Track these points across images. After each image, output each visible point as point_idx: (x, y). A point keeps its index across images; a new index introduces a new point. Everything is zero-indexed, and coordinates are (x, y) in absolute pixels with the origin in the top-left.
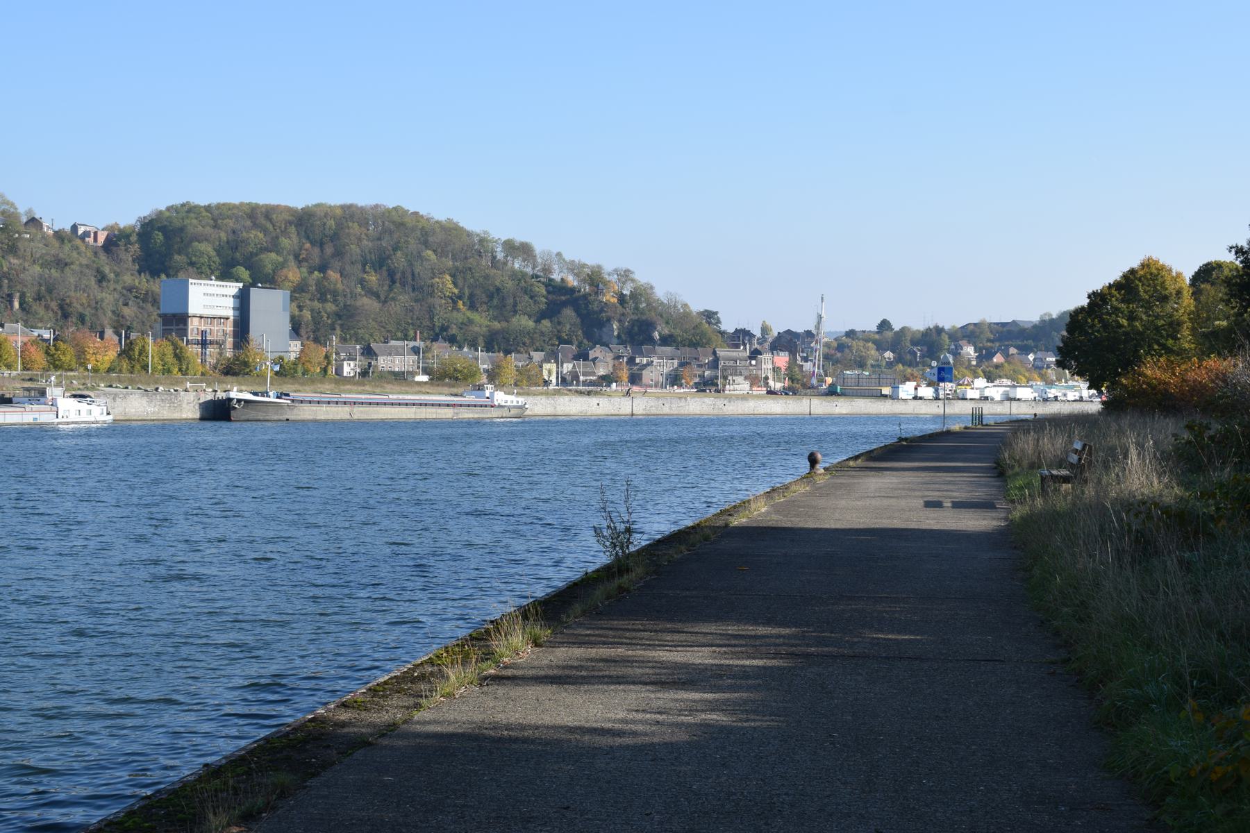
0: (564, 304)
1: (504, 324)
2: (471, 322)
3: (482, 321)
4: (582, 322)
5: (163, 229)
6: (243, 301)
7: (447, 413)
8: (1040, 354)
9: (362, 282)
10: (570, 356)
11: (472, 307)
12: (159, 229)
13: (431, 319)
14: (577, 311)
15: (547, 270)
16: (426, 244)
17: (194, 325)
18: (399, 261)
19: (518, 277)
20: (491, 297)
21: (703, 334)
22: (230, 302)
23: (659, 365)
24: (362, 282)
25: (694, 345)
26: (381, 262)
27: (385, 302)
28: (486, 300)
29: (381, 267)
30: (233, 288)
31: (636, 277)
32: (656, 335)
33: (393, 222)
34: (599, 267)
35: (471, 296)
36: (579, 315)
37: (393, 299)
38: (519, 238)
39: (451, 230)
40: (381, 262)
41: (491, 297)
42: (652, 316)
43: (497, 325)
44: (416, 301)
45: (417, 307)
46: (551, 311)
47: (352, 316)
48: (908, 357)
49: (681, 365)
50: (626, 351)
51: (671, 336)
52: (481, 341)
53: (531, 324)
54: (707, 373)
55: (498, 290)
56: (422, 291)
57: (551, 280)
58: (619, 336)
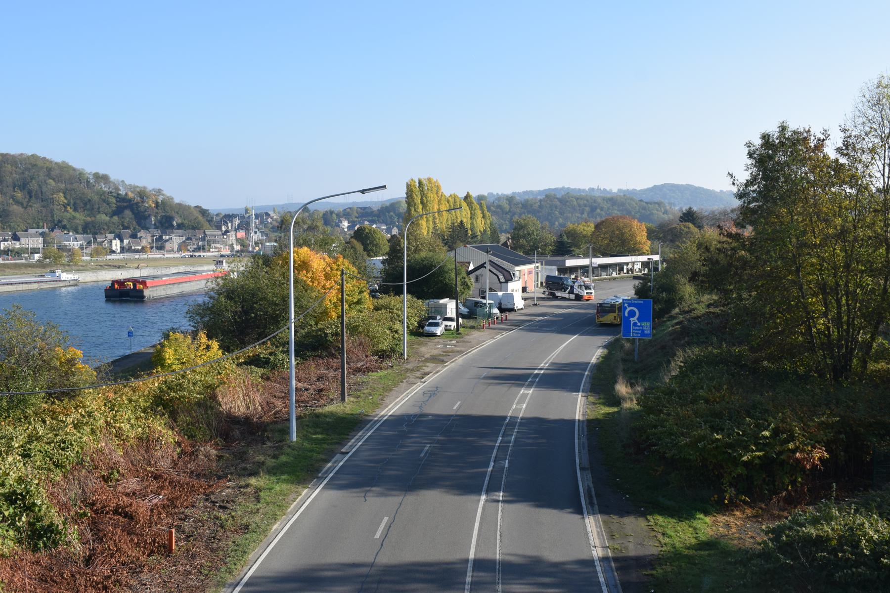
0: (126, 208)
1: (93, 219)
2: (74, 218)
3: (81, 217)
4: (136, 217)
7: (35, 286)
8: (378, 225)
9: (13, 197)
11: (75, 210)
13: (52, 216)
15: (117, 189)
16: (49, 176)
18: (34, 186)
19: (101, 194)
20: (85, 204)
21: (199, 223)
23: (176, 240)
24: (13, 197)
25: (194, 228)
26: (23, 186)
27: (26, 208)
28: (82, 205)
29: (24, 188)
31: (164, 192)
32: (175, 224)
33: (31, 164)
34: (145, 188)
35: (75, 204)
36: (133, 213)
37: (31, 206)
38: (102, 171)
39: (64, 168)
40: (23, 186)
41: (85, 204)
43: (89, 219)
44: (44, 207)
45: (44, 210)
46: (118, 212)
47: (7, 216)
49: (187, 239)
50: (158, 233)
51: (182, 224)
53: (108, 218)
55: (89, 200)
56: (47, 202)
57: (119, 194)
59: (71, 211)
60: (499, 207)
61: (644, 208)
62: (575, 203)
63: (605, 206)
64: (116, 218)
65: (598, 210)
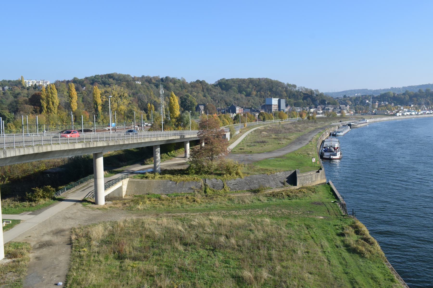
5: (224, 84)
12: (224, 84)
14: (310, 98)
17: (273, 106)
18: (274, 89)
22: (277, 102)
25: (334, 104)
26: (271, 90)
30: (277, 99)
42: (325, 99)
43: (295, 101)
53: (302, 101)
64: (305, 101)
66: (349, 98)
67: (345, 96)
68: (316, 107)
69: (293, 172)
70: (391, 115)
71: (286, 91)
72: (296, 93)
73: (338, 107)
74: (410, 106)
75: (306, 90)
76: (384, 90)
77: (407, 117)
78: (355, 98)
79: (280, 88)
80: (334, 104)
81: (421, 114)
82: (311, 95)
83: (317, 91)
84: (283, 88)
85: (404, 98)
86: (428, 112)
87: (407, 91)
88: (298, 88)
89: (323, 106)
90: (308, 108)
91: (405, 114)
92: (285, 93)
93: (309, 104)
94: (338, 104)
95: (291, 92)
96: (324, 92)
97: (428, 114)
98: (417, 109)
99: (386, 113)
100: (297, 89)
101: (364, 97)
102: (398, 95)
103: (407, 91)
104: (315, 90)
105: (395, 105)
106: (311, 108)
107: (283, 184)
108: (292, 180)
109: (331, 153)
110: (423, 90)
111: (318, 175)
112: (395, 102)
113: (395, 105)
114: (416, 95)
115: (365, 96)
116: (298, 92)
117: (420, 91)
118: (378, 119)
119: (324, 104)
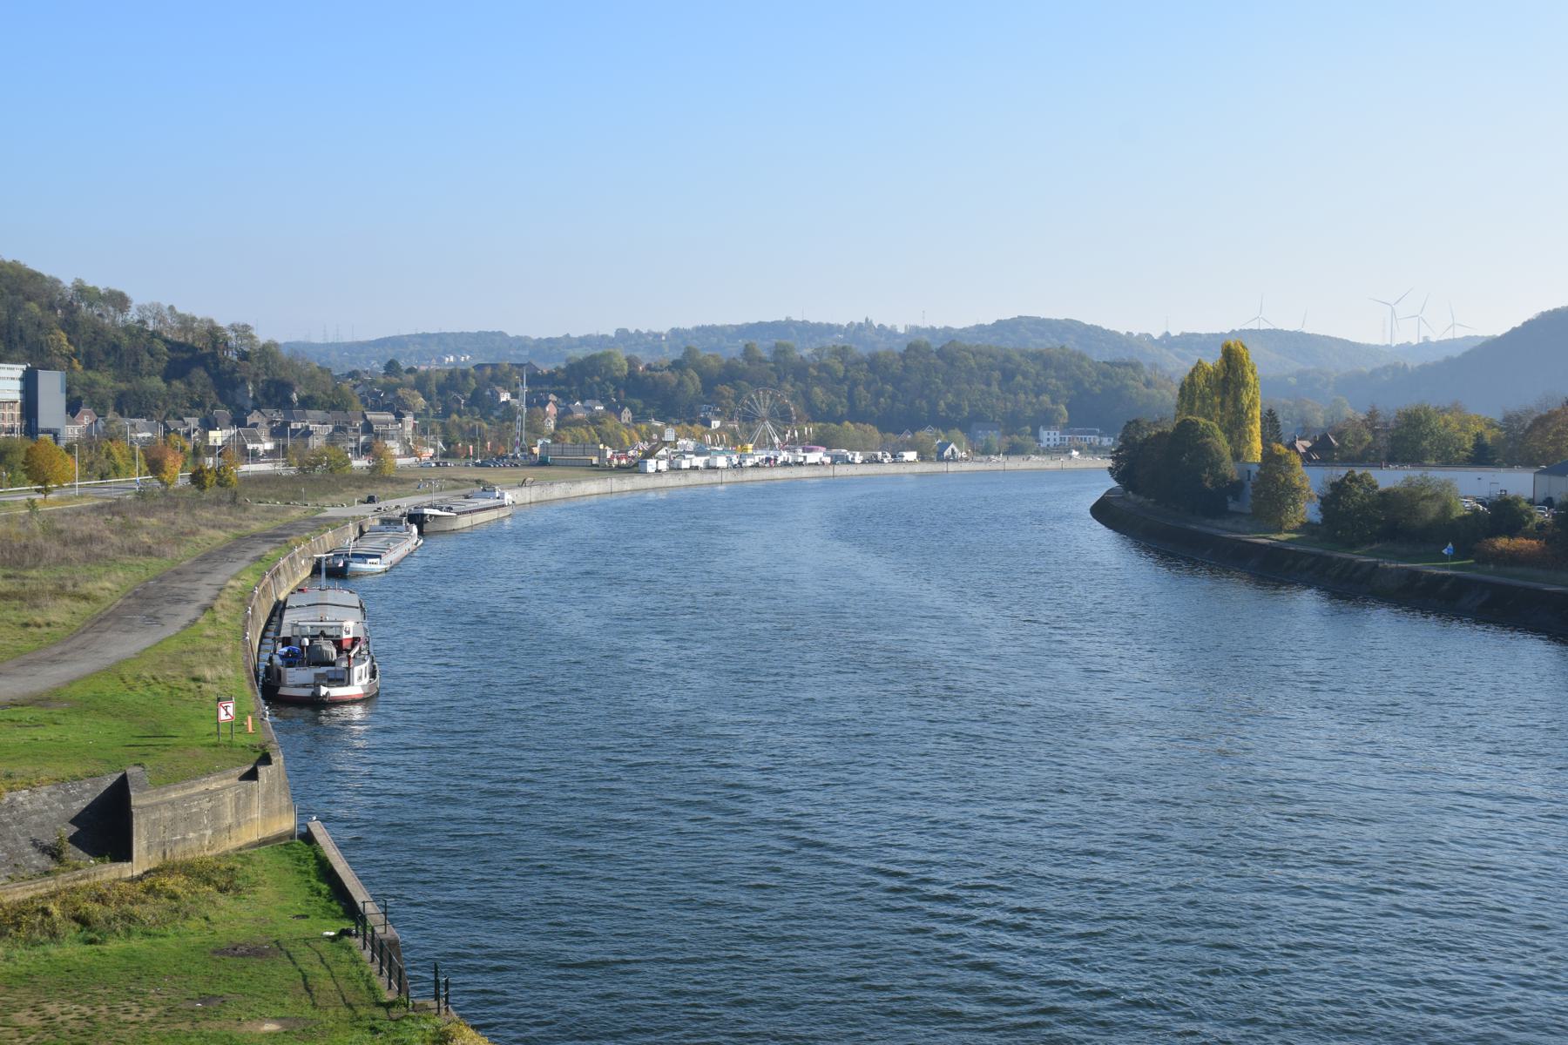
6: (29, 384)
10: (227, 422)
14: (207, 369)
22: (17, 385)
25: (334, 407)
30: (18, 370)
32: (294, 397)
36: (210, 375)
43: (123, 386)
48: (455, 406)
49: (336, 429)
51: (310, 397)
52: (110, 402)
53: (163, 386)
54: (362, 439)
58: (255, 398)
59: (79, 367)
60: (823, 367)
61: (1106, 375)
62: (973, 363)
63: (1032, 369)
64: (178, 385)
65: (1019, 378)
66: (411, 378)
67: (391, 367)
68: (239, 421)
69: (109, 781)
70: (620, 468)
71: (71, 325)
72: (126, 341)
73: (359, 424)
74: (707, 423)
75: (186, 323)
76: (585, 341)
77: (695, 478)
78: (442, 377)
79: (33, 306)
80: (335, 404)
81: (756, 466)
82: (213, 355)
83: (244, 331)
84: (52, 307)
85: (680, 383)
86: (784, 456)
87: (689, 352)
88: (141, 309)
89: (279, 417)
90: (193, 422)
91: (685, 464)
92: (63, 336)
93: (199, 405)
94: (357, 405)
95: (98, 332)
96: (281, 340)
97: (786, 464)
98: (735, 441)
99: (595, 460)
100: (132, 316)
101: (488, 371)
102: (648, 367)
103: (689, 352)
104: (233, 328)
105: (639, 417)
106: (209, 424)
107: (54, 853)
108: (106, 827)
109: (323, 670)
110: (764, 349)
111: (249, 794)
112: (638, 402)
113: (639, 417)
114: (730, 374)
115: (494, 366)
116: (137, 332)
117: (748, 351)
118: (558, 491)
119: (284, 404)
